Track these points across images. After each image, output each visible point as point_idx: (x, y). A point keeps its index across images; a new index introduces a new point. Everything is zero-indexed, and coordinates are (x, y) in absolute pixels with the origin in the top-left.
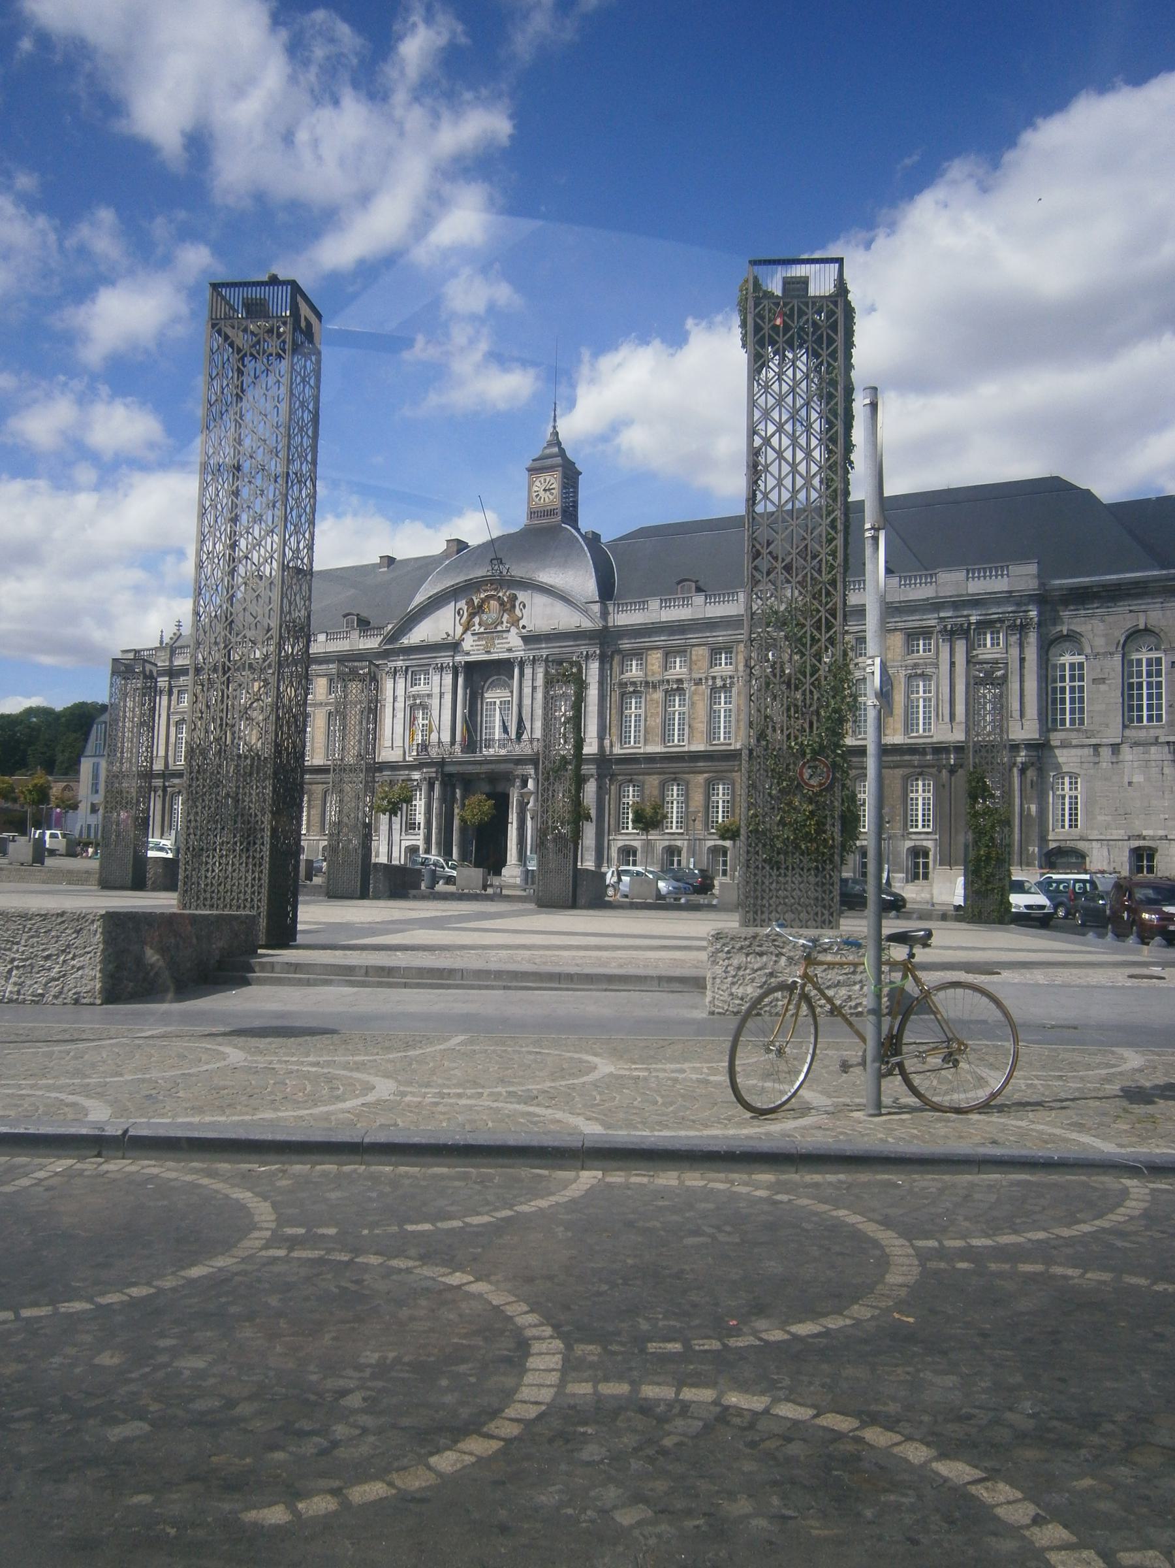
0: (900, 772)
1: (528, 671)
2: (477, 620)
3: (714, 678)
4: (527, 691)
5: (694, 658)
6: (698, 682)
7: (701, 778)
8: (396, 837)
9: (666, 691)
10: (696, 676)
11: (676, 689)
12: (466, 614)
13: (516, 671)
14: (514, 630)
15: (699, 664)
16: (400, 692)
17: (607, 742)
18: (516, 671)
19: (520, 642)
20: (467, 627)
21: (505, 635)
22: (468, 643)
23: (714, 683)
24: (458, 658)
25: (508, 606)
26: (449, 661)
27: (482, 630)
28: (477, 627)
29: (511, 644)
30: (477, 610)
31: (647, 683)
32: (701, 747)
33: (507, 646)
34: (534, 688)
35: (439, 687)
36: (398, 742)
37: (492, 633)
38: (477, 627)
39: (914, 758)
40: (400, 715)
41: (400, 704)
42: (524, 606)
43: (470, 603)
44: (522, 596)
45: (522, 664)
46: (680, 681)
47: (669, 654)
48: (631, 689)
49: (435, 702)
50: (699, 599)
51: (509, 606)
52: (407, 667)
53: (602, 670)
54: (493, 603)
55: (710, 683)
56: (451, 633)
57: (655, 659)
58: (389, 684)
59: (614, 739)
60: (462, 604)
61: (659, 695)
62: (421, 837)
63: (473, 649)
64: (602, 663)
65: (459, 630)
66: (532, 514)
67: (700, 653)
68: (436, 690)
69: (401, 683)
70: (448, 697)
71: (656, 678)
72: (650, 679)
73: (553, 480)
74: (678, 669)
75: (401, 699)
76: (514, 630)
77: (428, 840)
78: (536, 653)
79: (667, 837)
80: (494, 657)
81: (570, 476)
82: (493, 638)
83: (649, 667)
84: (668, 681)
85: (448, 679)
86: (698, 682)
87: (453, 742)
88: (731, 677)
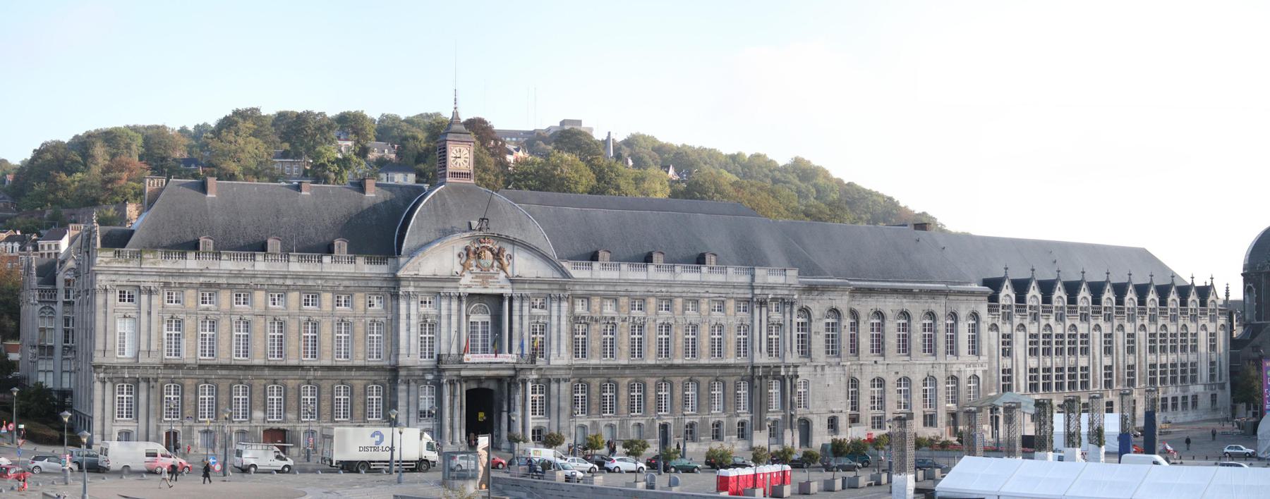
1: (516, 305)
6: (624, 320)
7: (626, 381)
13: (506, 304)
18: (506, 304)
20: (465, 267)
22: (467, 279)
24: (461, 290)
26: (453, 291)
32: (625, 362)
34: (521, 317)
43: (467, 249)
44: (508, 250)
45: (511, 299)
46: (613, 318)
49: (444, 322)
51: (497, 256)
54: (488, 253)
58: (403, 305)
63: (469, 283)
65: (459, 269)
70: (454, 319)
71: (597, 315)
76: (502, 275)
80: (489, 291)
85: (454, 305)
86: (624, 320)
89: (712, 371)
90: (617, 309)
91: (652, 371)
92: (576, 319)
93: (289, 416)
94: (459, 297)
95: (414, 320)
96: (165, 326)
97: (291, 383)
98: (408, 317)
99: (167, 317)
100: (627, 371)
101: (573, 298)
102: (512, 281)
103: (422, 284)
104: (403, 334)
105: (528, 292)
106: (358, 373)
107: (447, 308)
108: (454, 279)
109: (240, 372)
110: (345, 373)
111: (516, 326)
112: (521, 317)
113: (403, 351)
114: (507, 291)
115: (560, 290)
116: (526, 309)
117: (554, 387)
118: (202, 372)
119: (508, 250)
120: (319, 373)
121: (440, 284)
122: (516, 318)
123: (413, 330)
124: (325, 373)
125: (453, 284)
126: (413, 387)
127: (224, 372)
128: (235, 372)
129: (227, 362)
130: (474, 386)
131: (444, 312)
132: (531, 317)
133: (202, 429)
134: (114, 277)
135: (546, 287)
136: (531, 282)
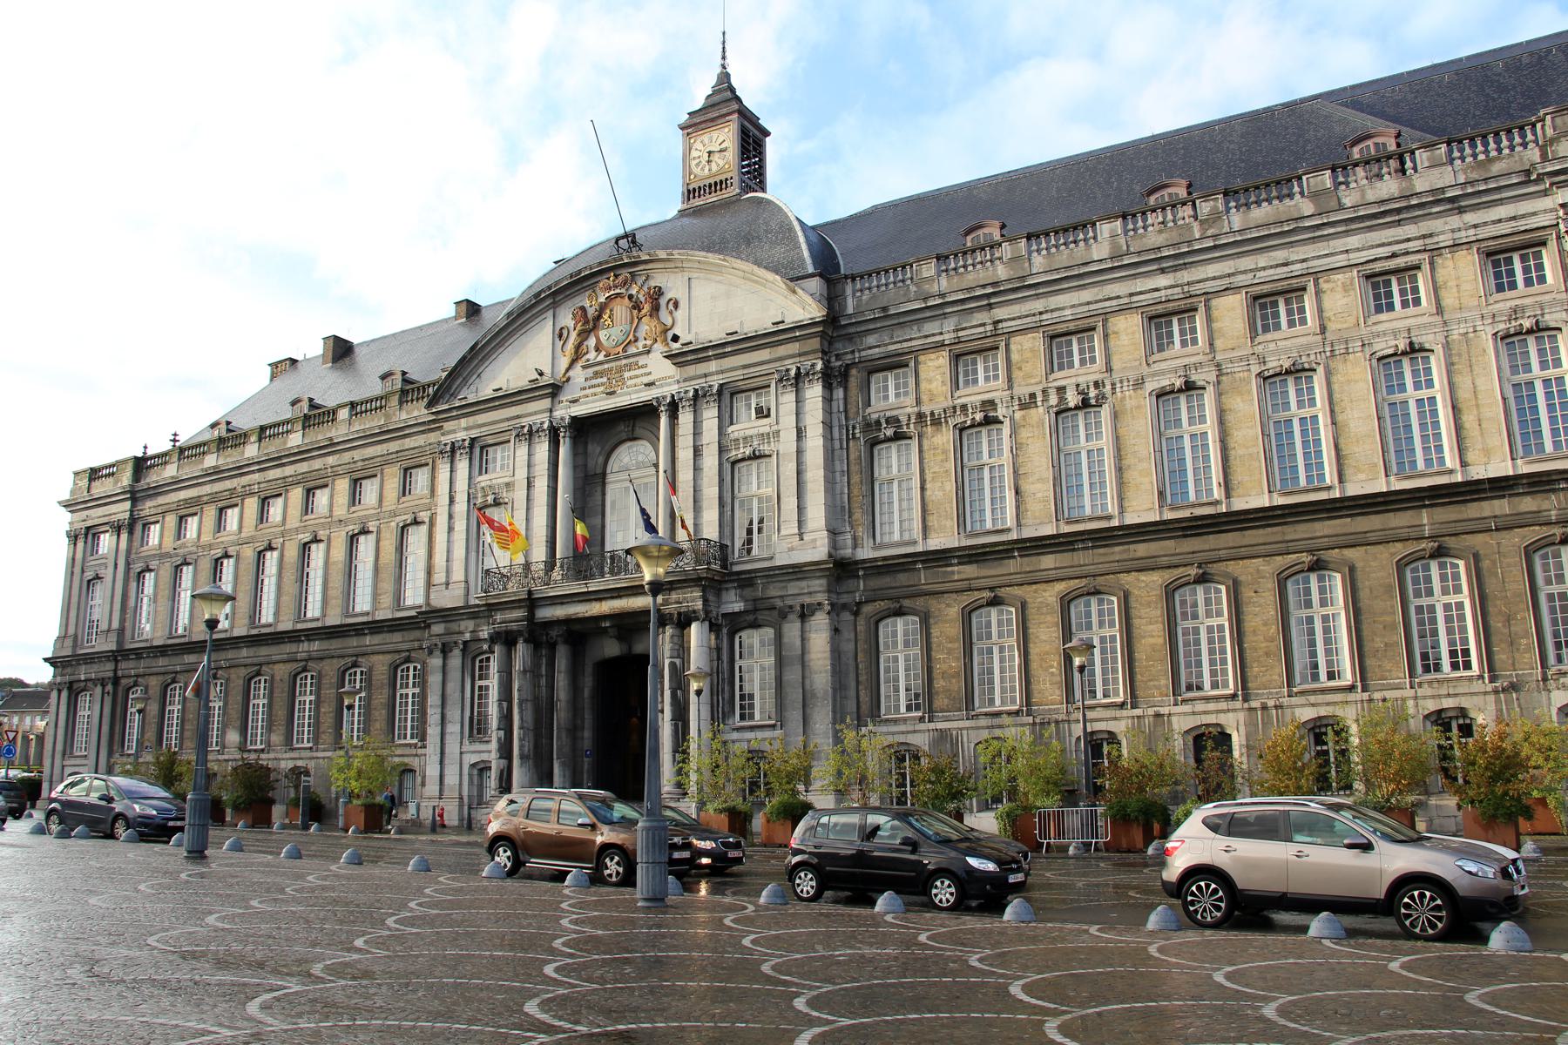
0: (1517, 539)
2: (592, 342)
3: (1061, 390)
4: (685, 454)
5: (1015, 357)
6: (1029, 403)
7: (1050, 595)
8: (452, 747)
9: (962, 429)
10: (1026, 391)
12: (574, 335)
15: (1027, 368)
17: (848, 539)
19: (668, 368)
21: (642, 360)
23: (1062, 399)
25: (647, 308)
27: (601, 358)
28: (592, 355)
29: (655, 377)
30: (590, 324)
31: (920, 416)
33: (646, 380)
34: (697, 452)
35: (526, 476)
36: (458, 574)
38: (592, 355)
39: (1545, 505)
40: (460, 526)
41: (461, 506)
42: (676, 305)
45: (674, 408)
46: (990, 404)
47: (962, 356)
48: (890, 432)
52: (473, 440)
53: (828, 400)
55: (1053, 400)
56: (547, 370)
59: (860, 531)
60: (567, 319)
61: (944, 438)
62: (494, 745)
64: (828, 387)
66: (690, 193)
67: (1029, 348)
68: (521, 474)
69: (462, 466)
70: (541, 485)
72: (926, 409)
73: (725, 137)
74: (985, 385)
75: (461, 499)
77: (506, 751)
78: (699, 383)
79: (983, 722)
81: (752, 140)
82: (620, 370)
83: (923, 386)
84: (964, 407)
85: (542, 449)
86: (1029, 403)
87: (550, 564)
88: (1096, 384)
89: (1399, 520)
91: (1142, 549)
94: (554, 434)
100: (1048, 561)
106: (377, 639)
110: (354, 642)
112: (697, 452)
120: (316, 645)
124: (325, 645)
125: (546, 403)
135: (764, 355)
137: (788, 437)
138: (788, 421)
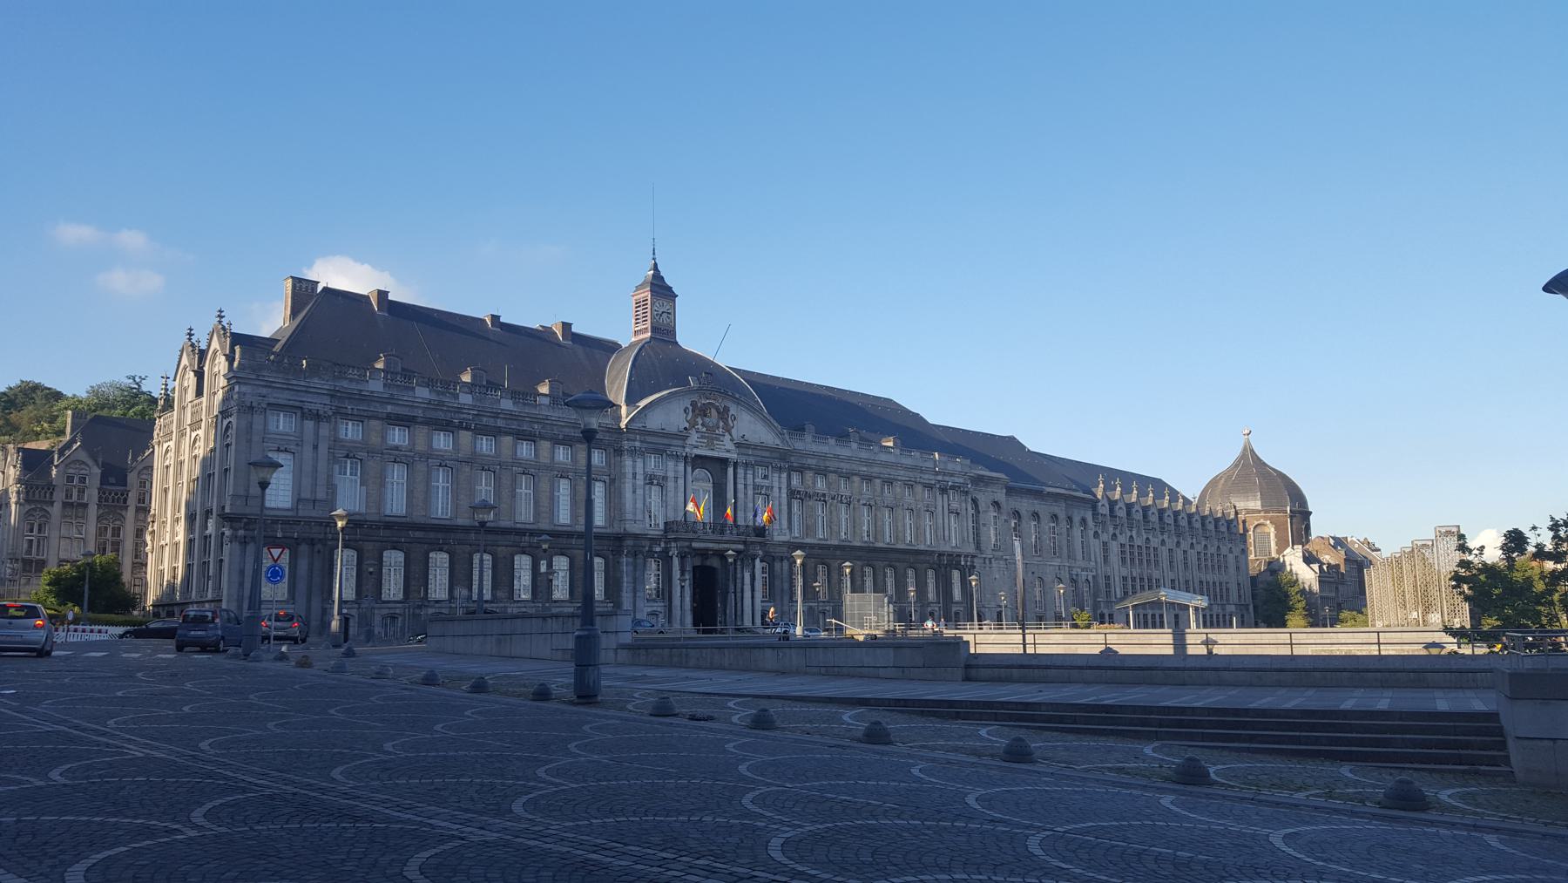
1: (740, 471)
11: (822, 498)
13: (731, 471)
14: (727, 437)
16: (639, 471)
18: (731, 471)
20: (693, 425)
22: (694, 438)
26: (680, 450)
37: (711, 437)
43: (693, 404)
49: (671, 484)
50: (832, 441)
51: (723, 414)
54: (714, 412)
57: (809, 475)
58: (628, 462)
63: (696, 445)
70: (681, 482)
71: (810, 491)
76: (727, 437)
85: (681, 467)
90: (829, 485)
92: (792, 494)
93: (499, 594)
95: (640, 481)
96: (337, 467)
97: (502, 551)
98: (634, 475)
99: (340, 453)
101: (791, 469)
102: (738, 445)
103: (649, 439)
104: (628, 495)
105: (752, 459)
107: (673, 468)
108: (682, 436)
109: (440, 535)
111: (741, 495)
113: (629, 516)
114: (733, 456)
115: (784, 461)
116: (750, 477)
117: (777, 565)
118: (388, 533)
119: (732, 412)
121: (666, 441)
122: (740, 487)
123: (640, 492)
126: (640, 561)
127: (418, 534)
128: (432, 535)
129: (422, 520)
130: (698, 562)
131: (671, 474)
132: (756, 487)
133: (385, 612)
134: (264, 391)
135: (767, 454)
136: (755, 447)
137: (776, 490)
138: (776, 484)
